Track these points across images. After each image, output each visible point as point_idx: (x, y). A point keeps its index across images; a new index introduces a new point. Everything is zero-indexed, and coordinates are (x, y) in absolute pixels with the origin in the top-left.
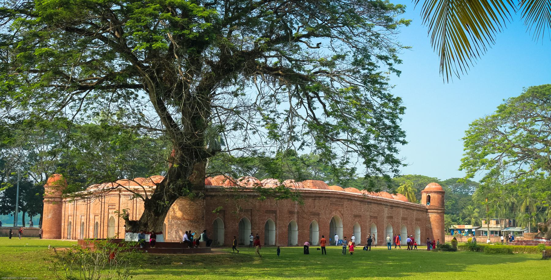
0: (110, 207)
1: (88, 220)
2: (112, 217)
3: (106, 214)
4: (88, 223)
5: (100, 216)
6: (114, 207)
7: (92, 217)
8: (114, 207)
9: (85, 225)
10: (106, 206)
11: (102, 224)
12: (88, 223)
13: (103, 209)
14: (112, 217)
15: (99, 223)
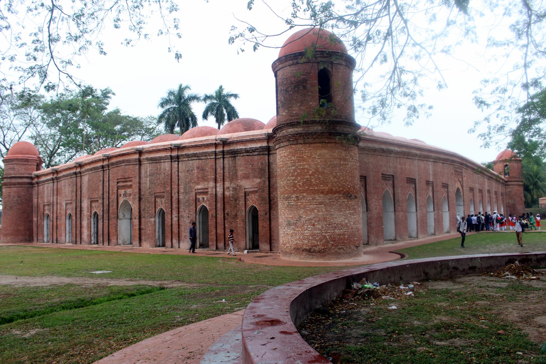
0: (120, 184)
1: (78, 209)
2: (126, 203)
3: (113, 197)
4: (78, 216)
5: (100, 201)
6: (129, 184)
7: (85, 204)
8: (129, 184)
9: (74, 218)
10: (113, 184)
11: (106, 216)
12: (78, 216)
13: (106, 189)
14: (126, 203)
15: (100, 213)
